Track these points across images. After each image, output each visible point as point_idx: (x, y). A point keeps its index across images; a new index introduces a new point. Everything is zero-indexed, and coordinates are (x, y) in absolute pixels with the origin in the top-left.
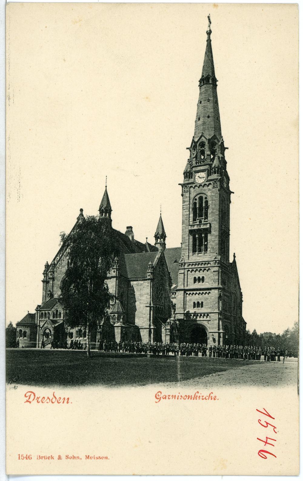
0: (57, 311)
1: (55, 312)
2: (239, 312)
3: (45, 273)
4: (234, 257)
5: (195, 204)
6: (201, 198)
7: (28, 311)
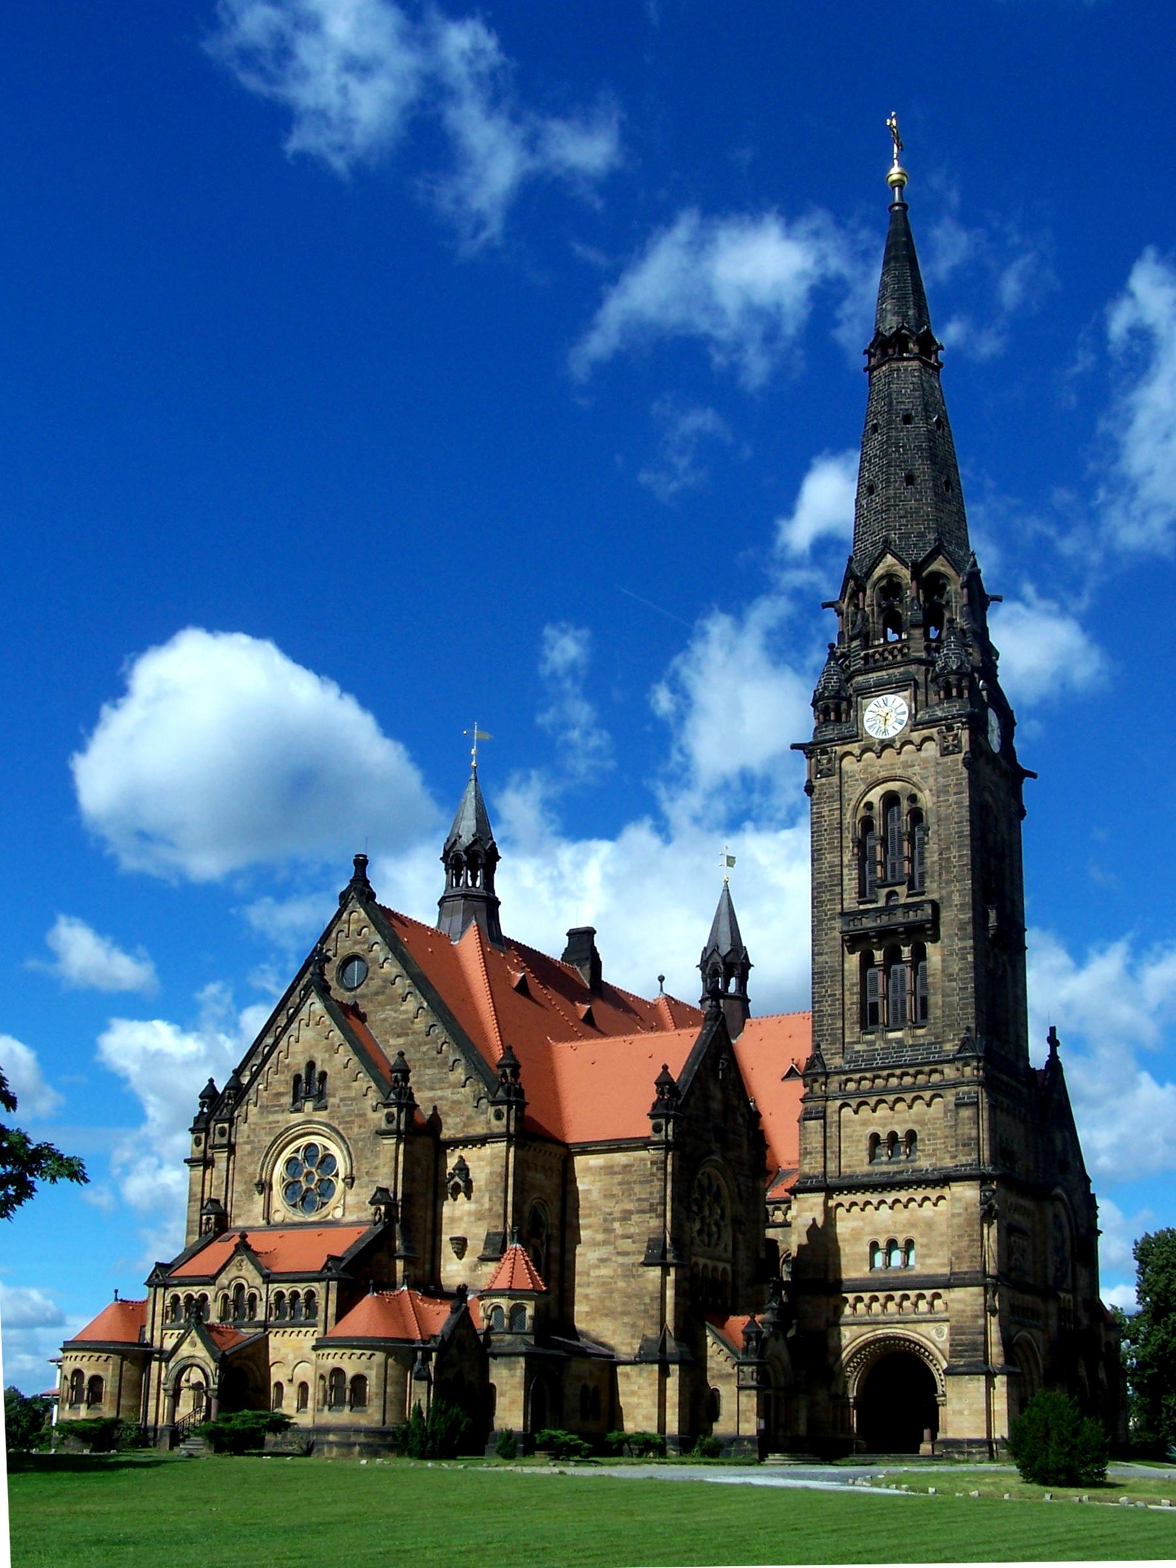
0: (240, 1288)
1: (231, 1294)
2: (1083, 1281)
3: (201, 1126)
4: (1053, 1041)
6: (891, 800)
7: (116, 1291)
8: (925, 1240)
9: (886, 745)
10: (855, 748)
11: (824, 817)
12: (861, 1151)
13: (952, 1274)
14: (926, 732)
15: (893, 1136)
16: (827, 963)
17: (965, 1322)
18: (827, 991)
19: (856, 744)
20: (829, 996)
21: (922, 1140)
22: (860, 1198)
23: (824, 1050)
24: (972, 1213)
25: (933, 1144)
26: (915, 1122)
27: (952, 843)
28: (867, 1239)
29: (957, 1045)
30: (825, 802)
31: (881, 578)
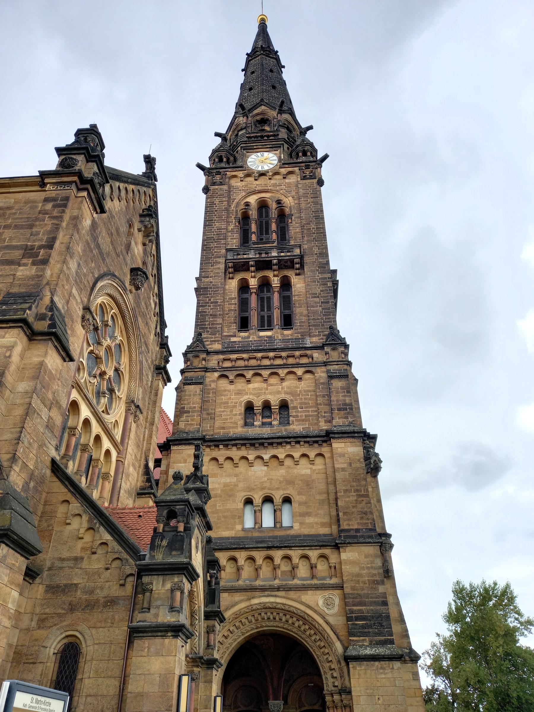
5: (245, 218)
6: (263, 206)
8: (303, 498)
9: (262, 174)
10: (241, 174)
11: (215, 204)
12: (236, 415)
13: (341, 531)
14: (291, 169)
15: (267, 406)
16: (211, 282)
17: (363, 589)
18: (210, 300)
19: (241, 172)
20: (212, 303)
21: (295, 408)
22: (235, 453)
23: (205, 338)
24: (357, 469)
25: (305, 411)
26: (286, 393)
27: (311, 221)
28: (241, 496)
29: (322, 339)
30: (217, 198)
31: (257, 114)
